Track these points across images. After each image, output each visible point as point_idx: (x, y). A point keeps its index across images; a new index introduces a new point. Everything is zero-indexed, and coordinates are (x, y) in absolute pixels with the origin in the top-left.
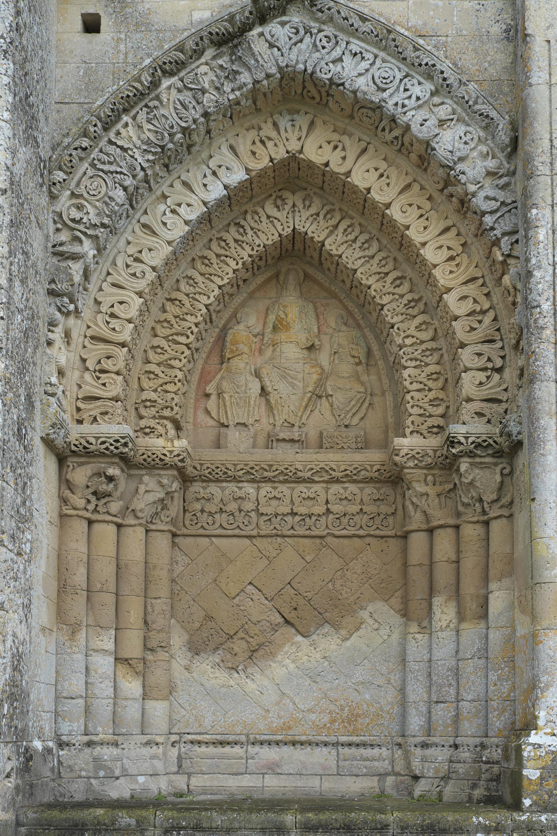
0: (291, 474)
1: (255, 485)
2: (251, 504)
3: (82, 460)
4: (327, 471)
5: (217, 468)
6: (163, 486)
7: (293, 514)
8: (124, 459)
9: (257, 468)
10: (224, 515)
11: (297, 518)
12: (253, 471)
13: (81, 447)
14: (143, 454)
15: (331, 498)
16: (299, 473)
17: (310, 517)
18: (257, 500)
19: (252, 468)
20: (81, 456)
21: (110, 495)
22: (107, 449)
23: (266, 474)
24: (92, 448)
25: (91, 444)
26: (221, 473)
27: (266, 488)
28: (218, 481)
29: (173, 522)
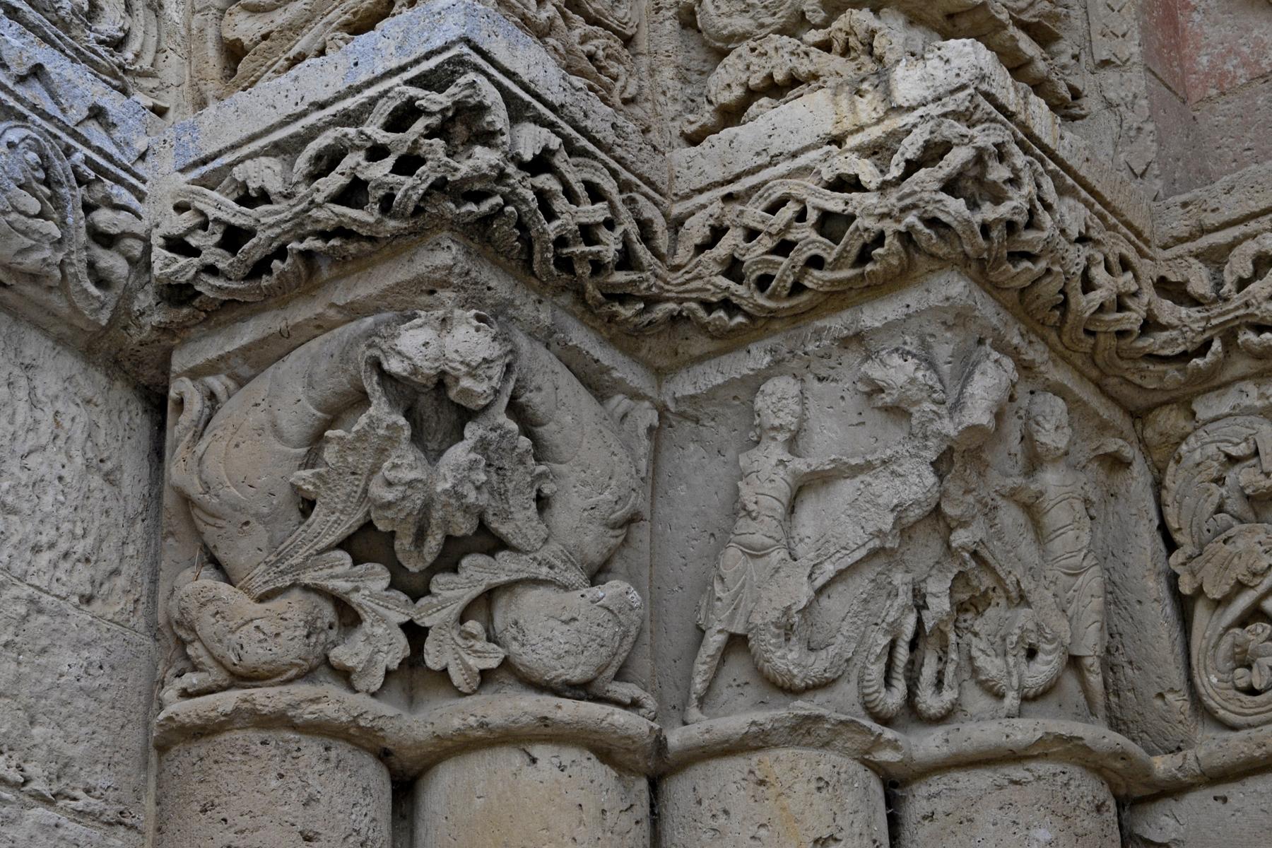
3: (249, 332)
6: (898, 412)
8: (510, 240)
13: (205, 241)
14: (718, 232)
20: (228, 310)
21: (491, 542)
22: (353, 193)
24: (267, 222)
25: (264, 197)
29: (1104, 679)
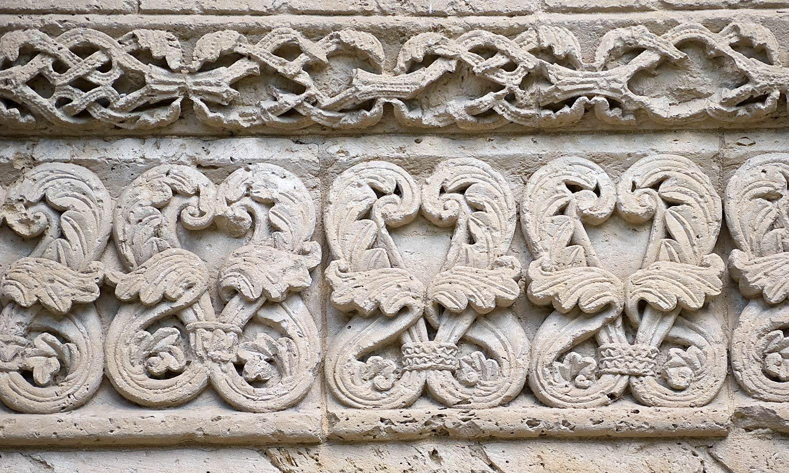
0: (511, 80)
1: (308, 153)
2: (286, 259)
4: (717, 61)
5: (84, 50)
7: (538, 310)
9: (319, 50)
10: (127, 324)
11: (557, 333)
12: (292, 67)
15: (745, 216)
16: (556, 71)
17: (631, 329)
18: (321, 235)
19: (288, 51)
23: (366, 82)
26: (105, 82)
27: (373, 163)
28: (87, 129)
